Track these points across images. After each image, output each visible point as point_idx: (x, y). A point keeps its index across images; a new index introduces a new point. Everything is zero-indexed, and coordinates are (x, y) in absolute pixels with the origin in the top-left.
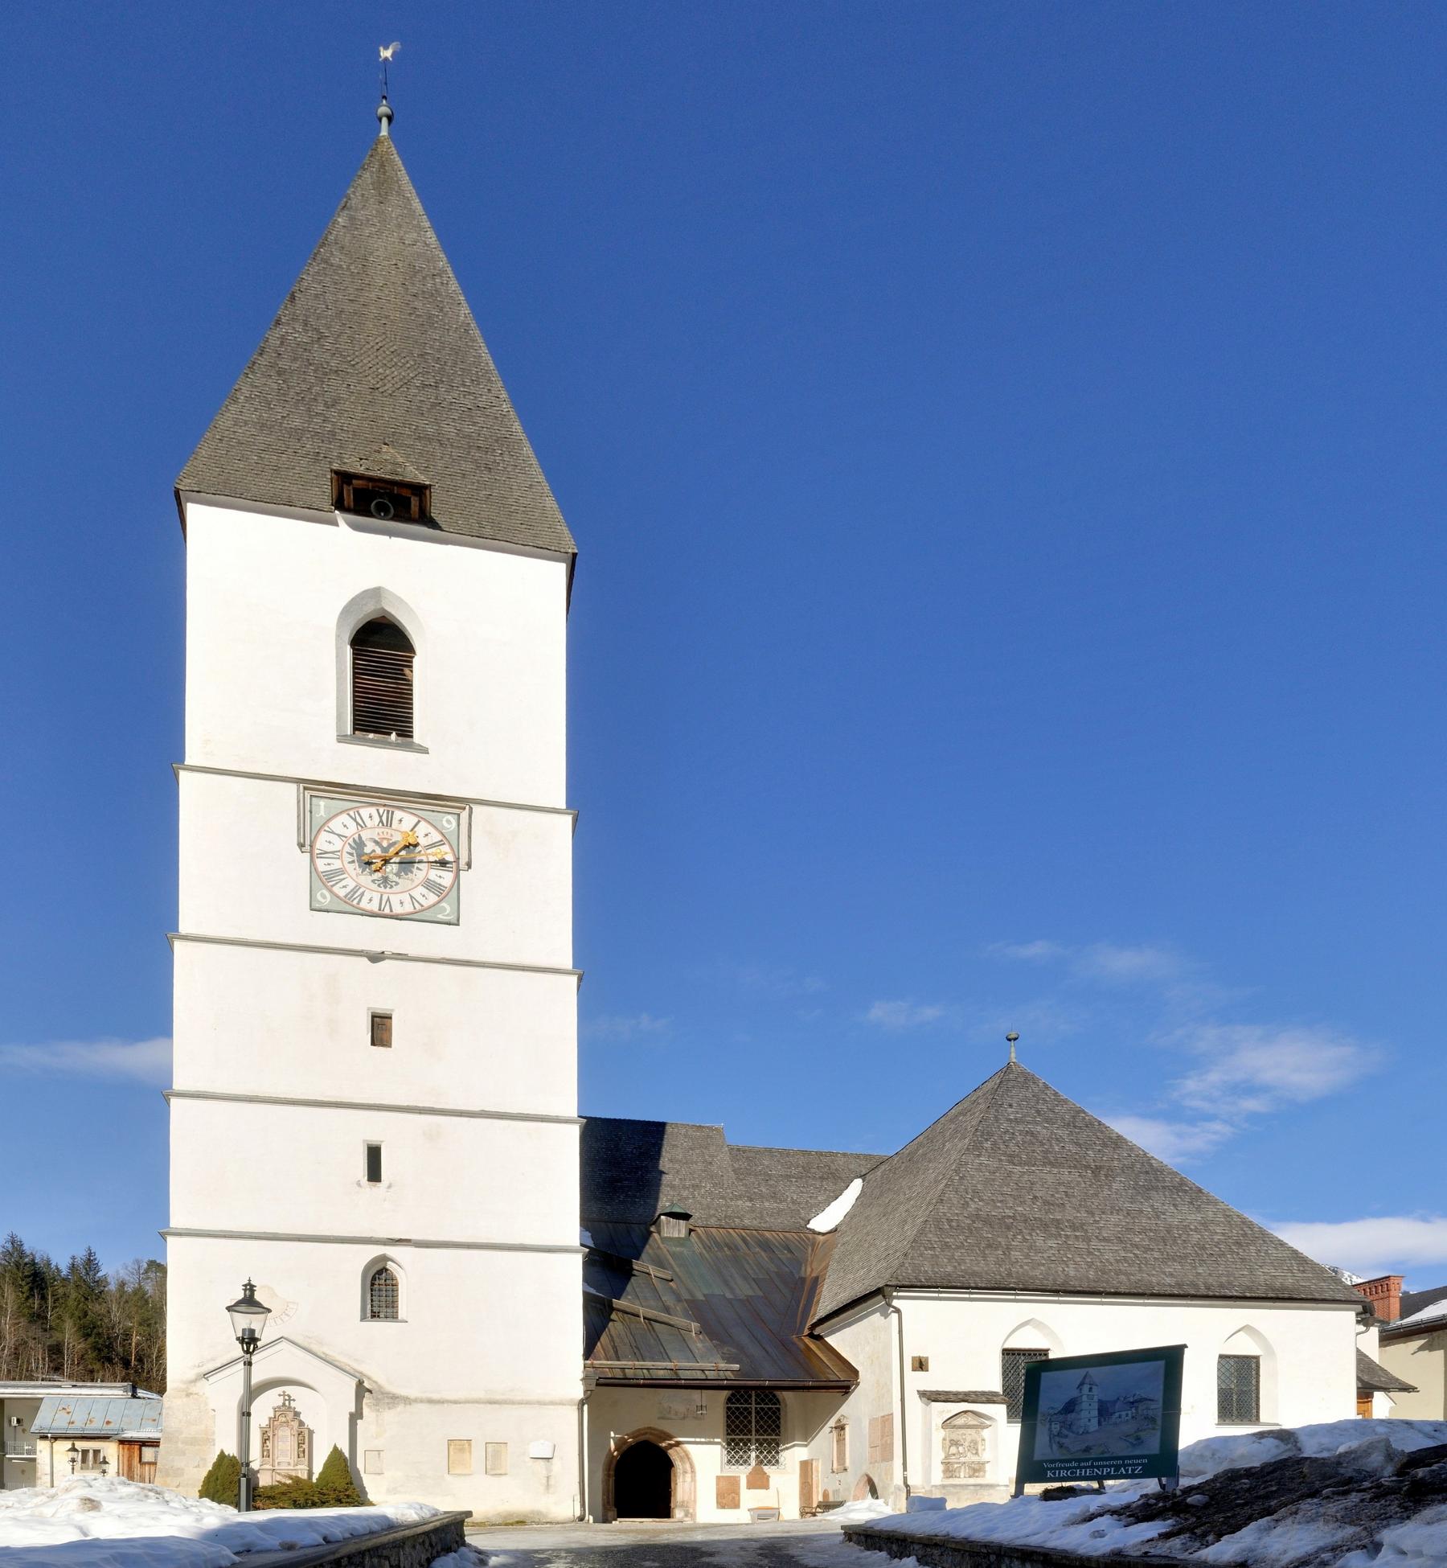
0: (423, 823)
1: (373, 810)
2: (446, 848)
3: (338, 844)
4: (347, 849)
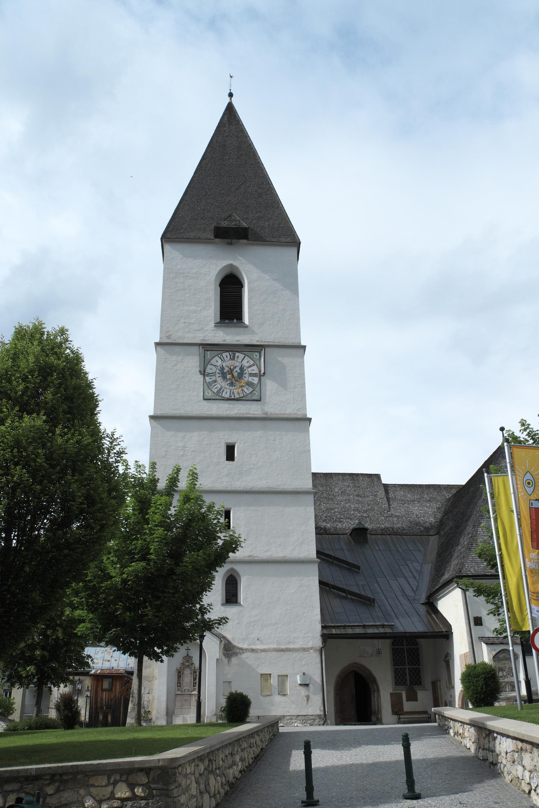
0: (246, 357)
1: (227, 354)
2: (255, 368)
3: (214, 369)
4: (218, 371)
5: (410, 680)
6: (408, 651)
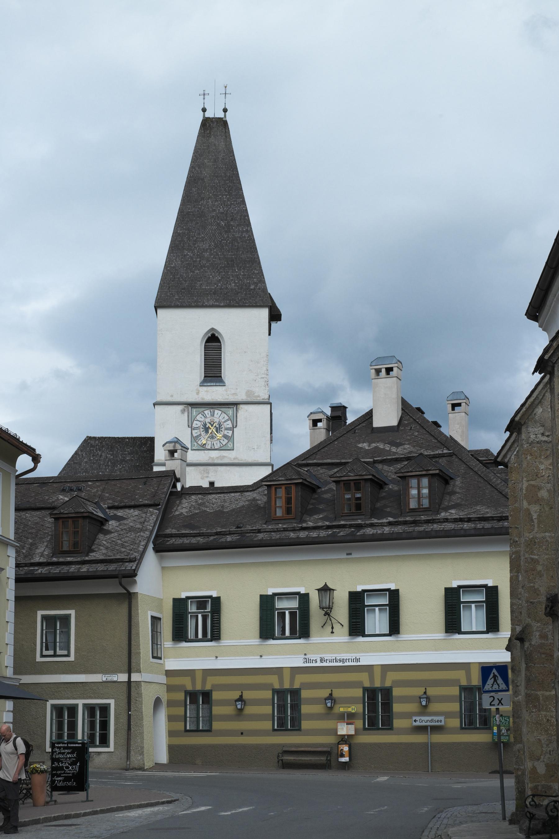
3: (199, 424)
4: (202, 426)
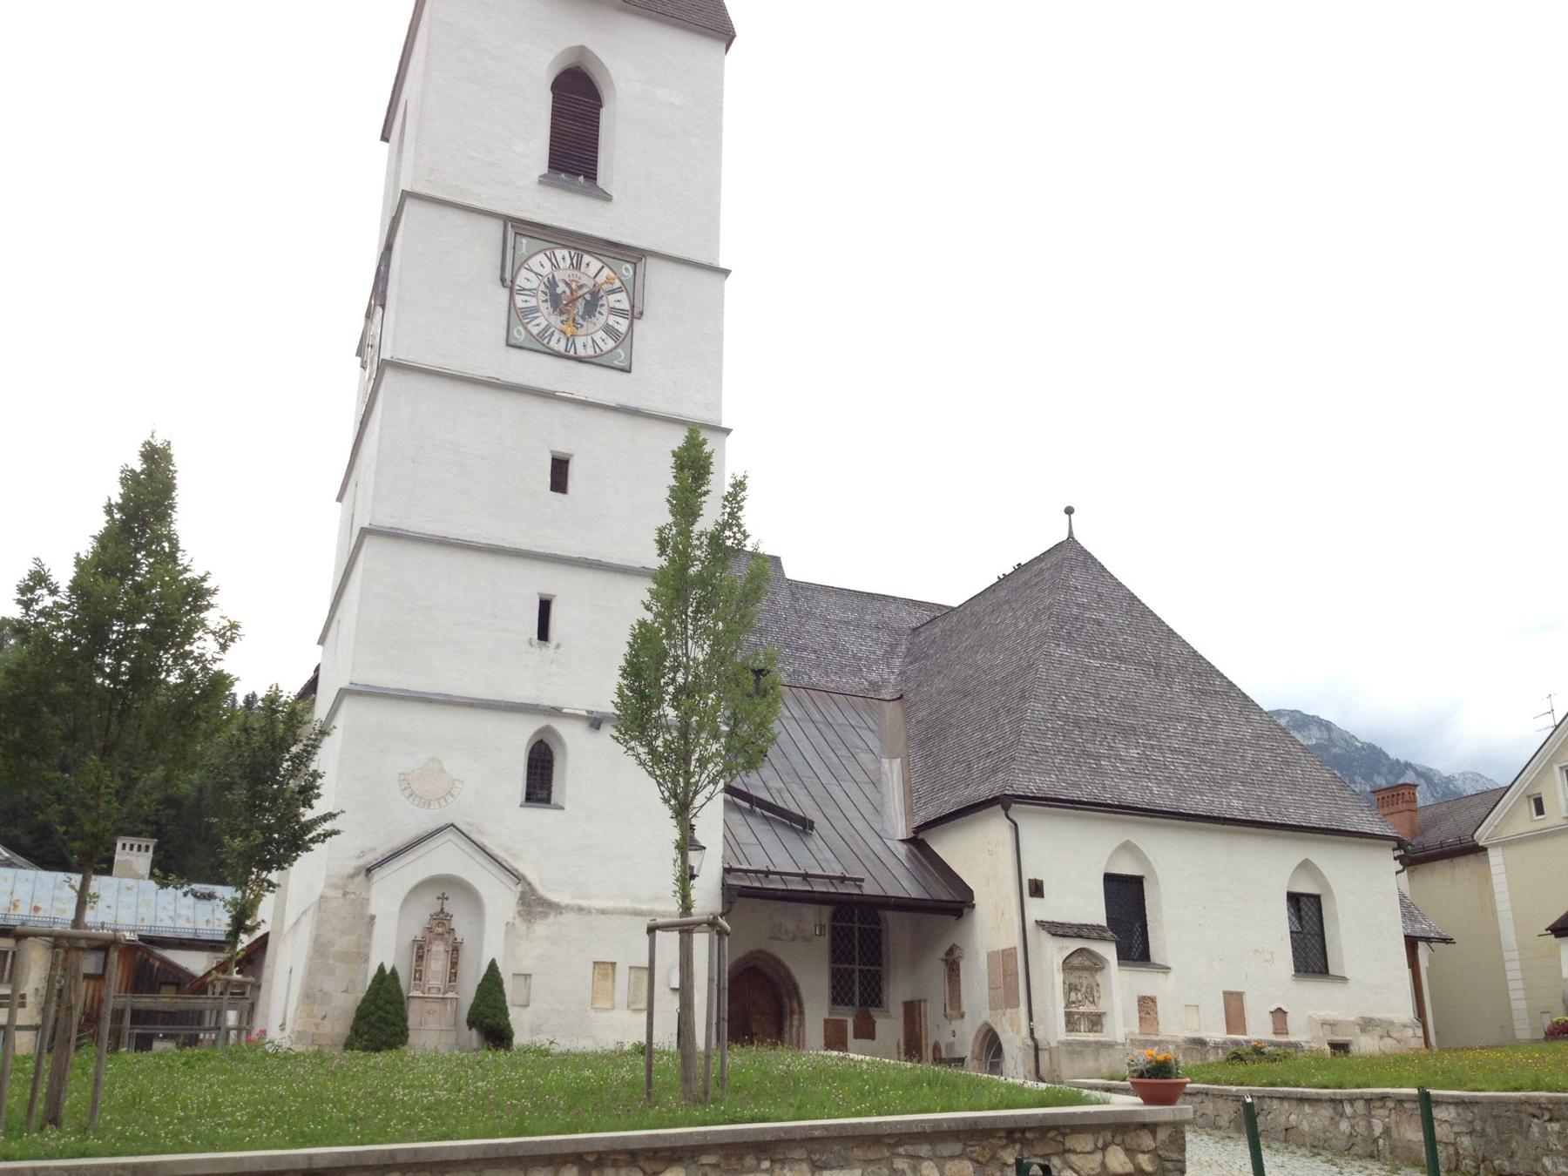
0: (606, 270)
1: (565, 252)
2: (622, 296)
4: (542, 288)
5: (861, 994)
6: (861, 935)
